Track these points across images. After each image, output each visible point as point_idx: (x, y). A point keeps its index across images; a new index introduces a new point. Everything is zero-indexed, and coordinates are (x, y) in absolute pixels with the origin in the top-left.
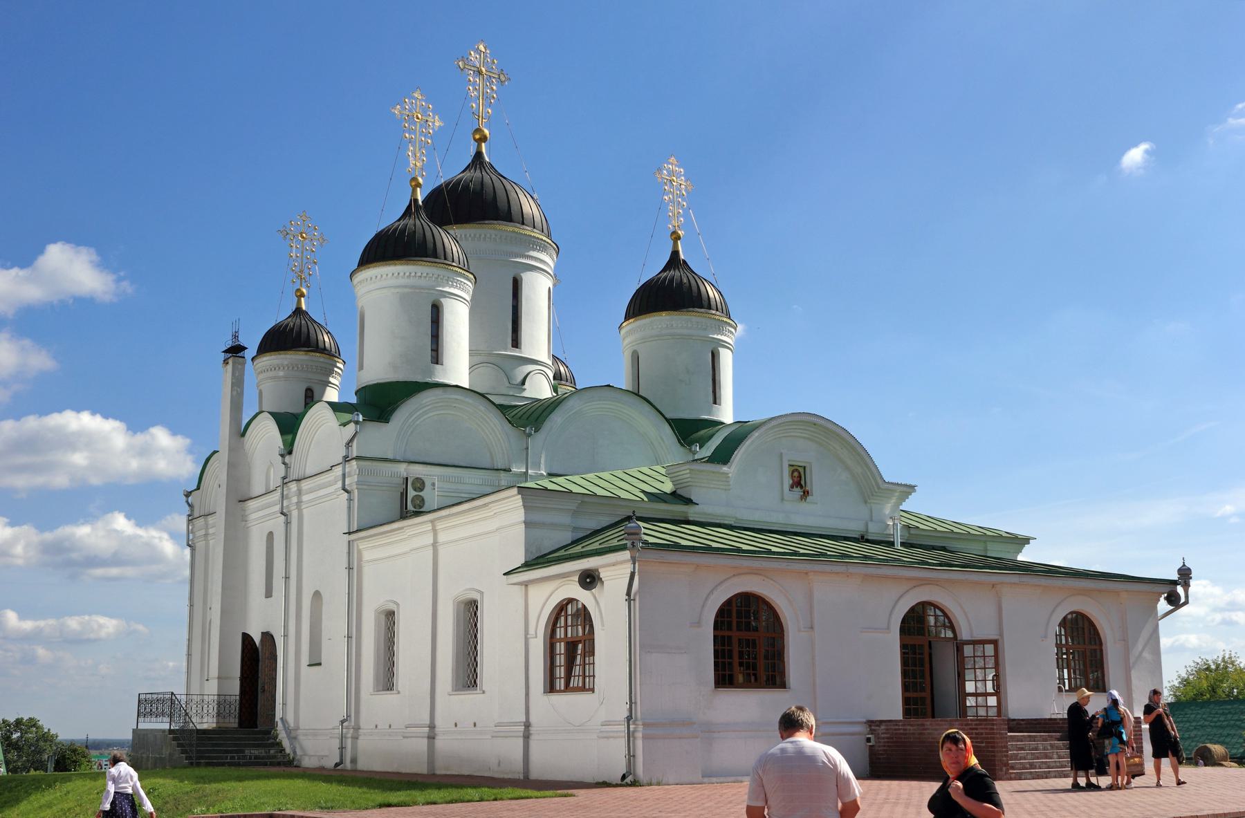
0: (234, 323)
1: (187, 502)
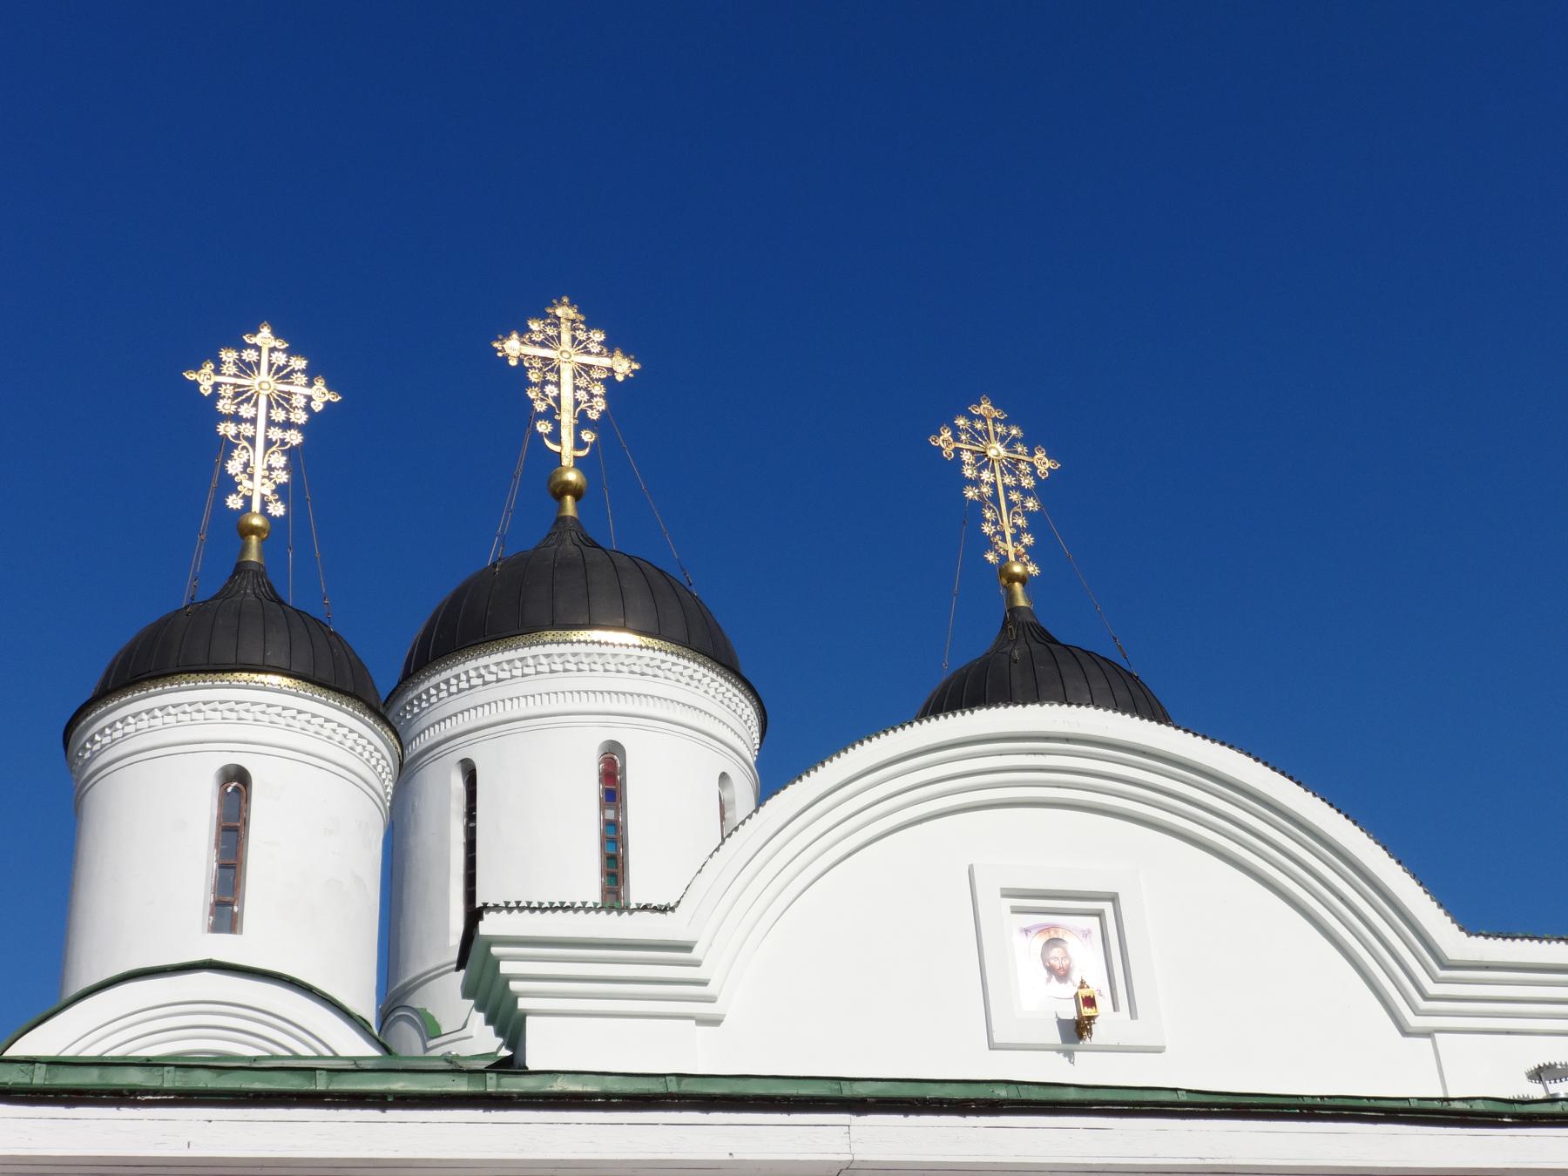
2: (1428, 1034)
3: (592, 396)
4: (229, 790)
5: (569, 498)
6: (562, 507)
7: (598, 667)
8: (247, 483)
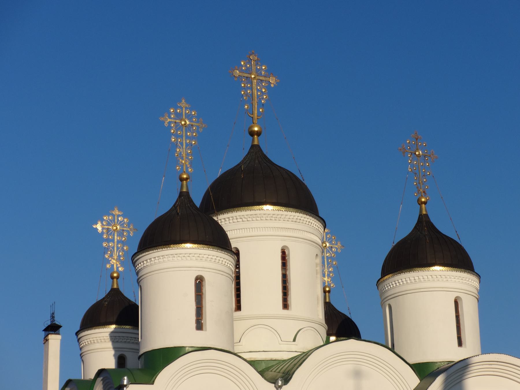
0: (52, 305)
4: (197, 282)
7: (282, 219)
8: (180, 160)
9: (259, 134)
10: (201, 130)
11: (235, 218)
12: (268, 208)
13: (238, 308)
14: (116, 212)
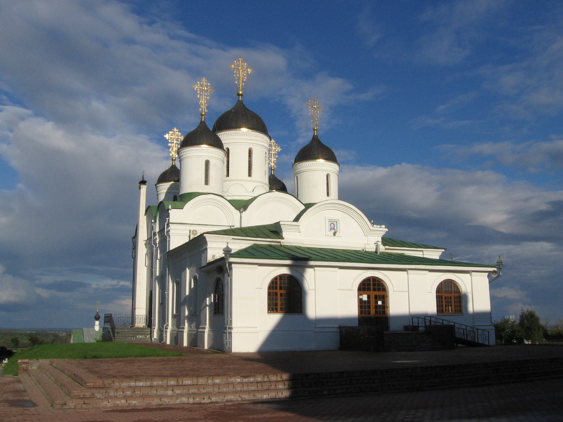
1: (133, 241)
2: (367, 236)
3: (244, 76)
5: (240, 96)
6: (239, 98)
8: (202, 106)
9: (242, 95)
10: (212, 92)
11: (228, 134)
12: (244, 130)
13: (228, 175)
14: (175, 130)
